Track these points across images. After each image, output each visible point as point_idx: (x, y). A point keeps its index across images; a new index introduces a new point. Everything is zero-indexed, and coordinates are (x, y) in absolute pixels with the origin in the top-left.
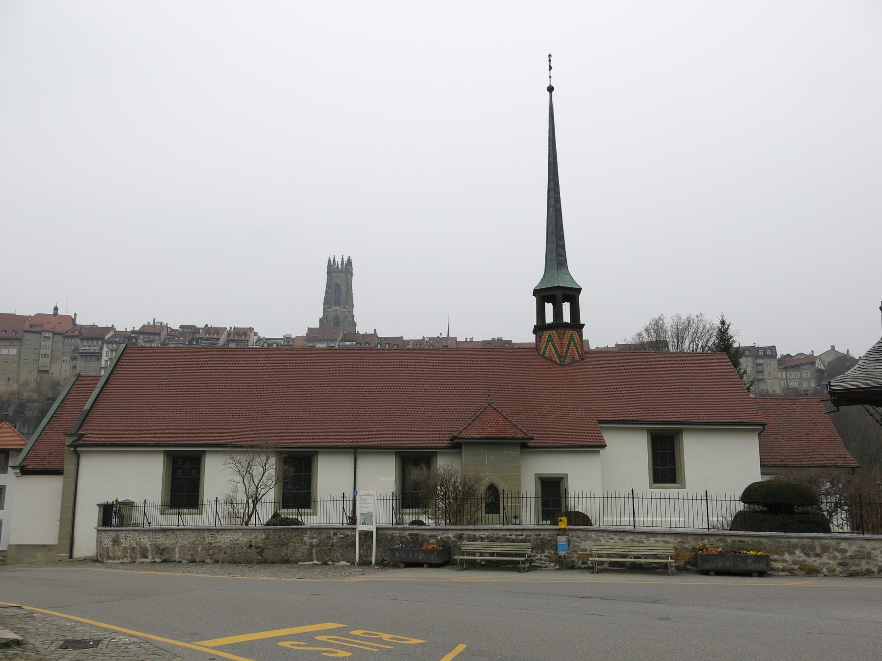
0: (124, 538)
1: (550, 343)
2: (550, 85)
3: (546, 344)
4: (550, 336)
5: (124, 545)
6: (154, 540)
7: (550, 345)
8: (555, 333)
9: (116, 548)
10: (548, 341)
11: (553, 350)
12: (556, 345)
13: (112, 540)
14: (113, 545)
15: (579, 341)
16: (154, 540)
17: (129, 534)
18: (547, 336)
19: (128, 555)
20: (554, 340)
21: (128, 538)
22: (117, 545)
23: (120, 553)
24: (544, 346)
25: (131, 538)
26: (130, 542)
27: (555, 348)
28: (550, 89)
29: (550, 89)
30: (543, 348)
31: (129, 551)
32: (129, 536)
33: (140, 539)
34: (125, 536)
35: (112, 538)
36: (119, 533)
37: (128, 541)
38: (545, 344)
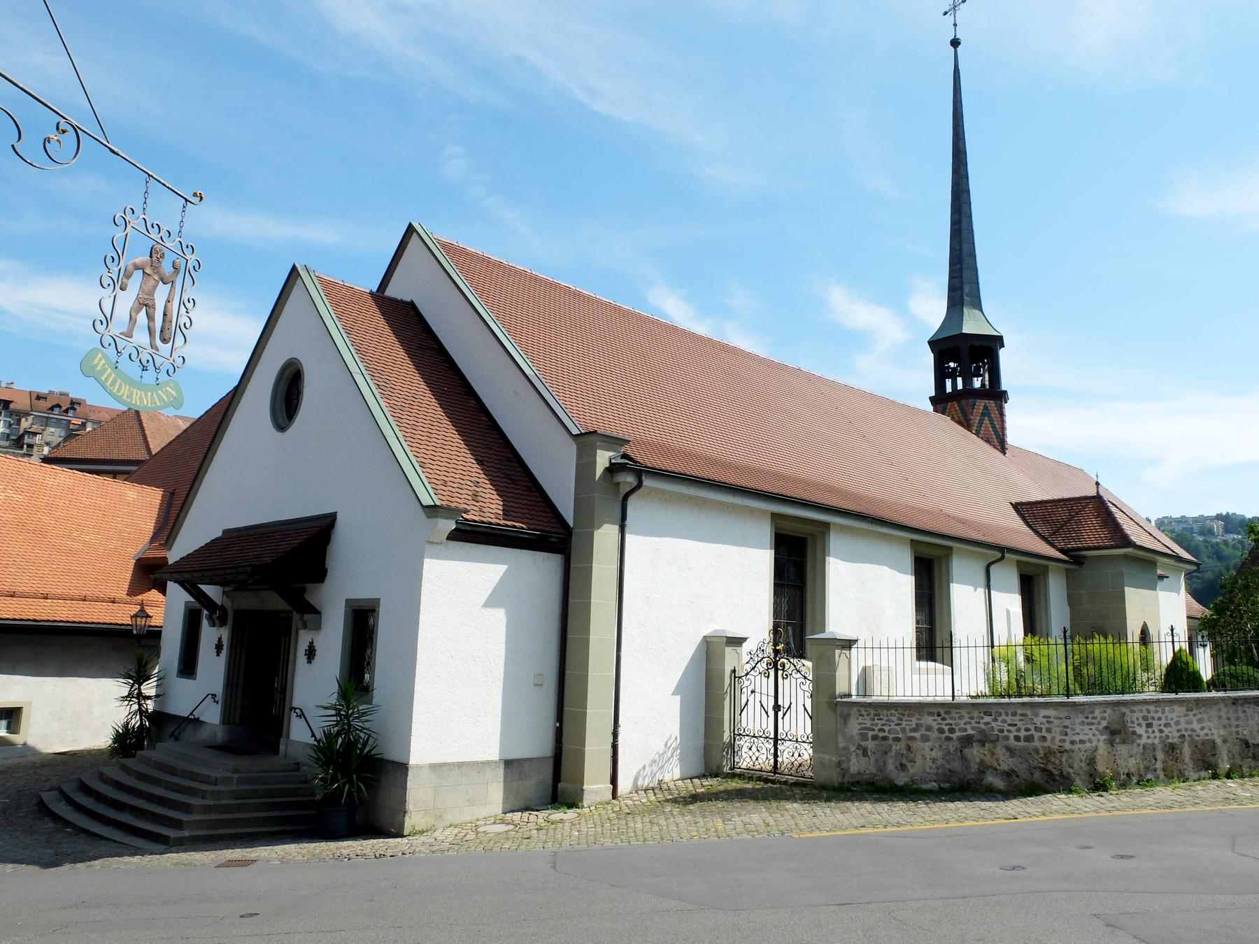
0: (1144, 724)
1: (986, 418)
2: (955, 36)
3: (980, 419)
4: (986, 408)
5: (1144, 740)
6: (1234, 723)
7: (986, 421)
8: (994, 405)
9: (1123, 749)
10: (983, 415)
11: (991, 429)
12: (995, 423)
13: (1106, 728)
14: (1111, 743)
16: (1234, 723)
17: (1157, 712)
18: (982, 408)
19: (1159, 765)
20: (993, 416)
21: (1155, 723)
22: (1124, 742)
23: (1133, 761)
24: (977, 421)
25: (1163, 722)
26: (1161, 731)
27: (994, 427)
28: (955, 43)
29: (955, 43)
30: (976, 425)
31: (1160, 755)
32: (1156, 716)
33: (1190, 722)
34: (1145, 718)
35: (1104, 724)
36: (1124, 709)
37: (1155, 728)
38: (979, 418)
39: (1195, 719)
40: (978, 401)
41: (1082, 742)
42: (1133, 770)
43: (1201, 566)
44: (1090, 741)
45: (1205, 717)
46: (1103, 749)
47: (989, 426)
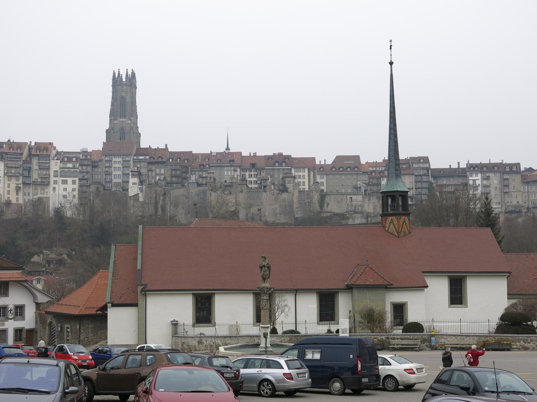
0: (205, 341)
1: (392, 224)
2: (391, 60)
3: (390, 224)
4: (392, 220)
5: (205, 344)
6: (224, 341)
7: (392, 225)
8: (395, 218)
9: (201, 345)
10: (390, 223)
11: (394, 228)
12: (396, 225)
13: (198, 341)
14: (199, 344)
15: (408, 222)
16: (224, 341)
17: (208, 339)
18: (390, 220)
19: (208, 349)
20: (394, 222)
21: (208, 341)
22: (201, 344)
23: (203, 348)
24: (388, 225)
25: (209, 341)
26: (209, 342)
27: (395, 227)
28: (391, 63)
29: (391, 63)
30: (387, 227)
31: (209, 347)
32: (208, 339)
33: (215, 341)
34: (206, 340)
35: (197, 341)
36: (201, 338)
37: (208, 342)
38: (389, 224)
39: (216, 340)
40: (389, 217)
41: (193, 344)
42: (203, 349)
43: (511, 274)
44: (195, 344)
45: (219, 340)
46: (197, 345)
47: (393, 227)
